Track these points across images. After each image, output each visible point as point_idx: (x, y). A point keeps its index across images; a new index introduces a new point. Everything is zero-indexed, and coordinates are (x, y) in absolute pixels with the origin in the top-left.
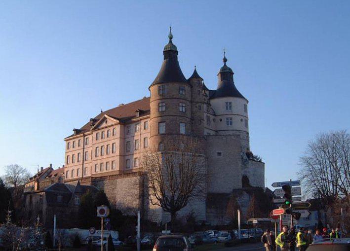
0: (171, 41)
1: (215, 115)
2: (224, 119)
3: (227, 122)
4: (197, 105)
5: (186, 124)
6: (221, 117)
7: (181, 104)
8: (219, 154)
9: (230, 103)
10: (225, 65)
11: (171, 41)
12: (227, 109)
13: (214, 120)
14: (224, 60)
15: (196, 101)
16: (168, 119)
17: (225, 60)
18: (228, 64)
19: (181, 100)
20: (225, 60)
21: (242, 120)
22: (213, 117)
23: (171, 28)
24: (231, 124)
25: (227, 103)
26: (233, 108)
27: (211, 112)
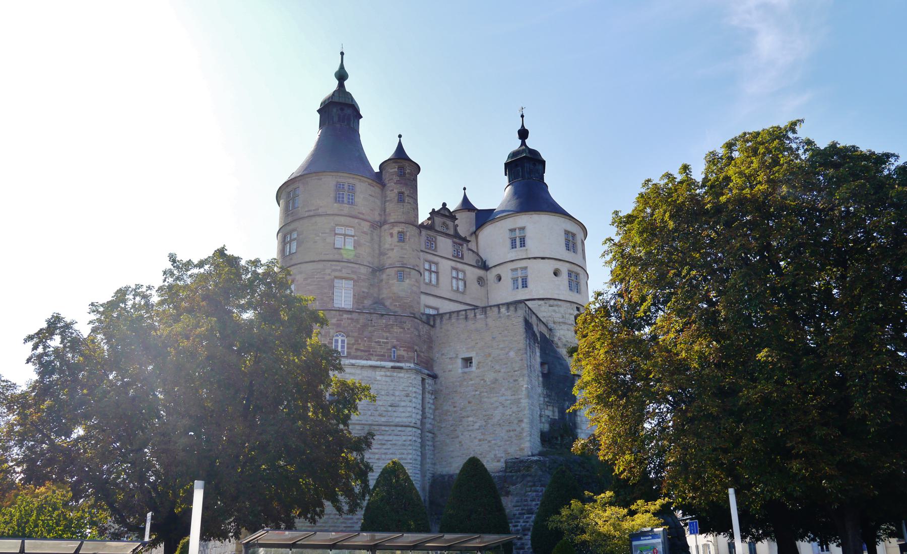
0: (341, 85)
1: (484, 266)
2: (506, 273)
3: (515, 280)
4: (396, 230)
5: (355, 281)
6: (497, 271)
7: (339, 230)
8: (468, 361)
9: (523, 229)
10: (523, 143)
11: (341, 85)
12: (513, 246)
13: (481, 281)
14: (519, 132)
15: (393, 221)
16: (301, 273)
17: (523, 134)
18: (531, 143)
19: (343, 220)
20: (523, 134)
21: (556, 273)
22: (481, 273)
23: (342, 54)
24: (525, 285)
25: (512, 230)
26: (528, 242)
27: (469, 258)
